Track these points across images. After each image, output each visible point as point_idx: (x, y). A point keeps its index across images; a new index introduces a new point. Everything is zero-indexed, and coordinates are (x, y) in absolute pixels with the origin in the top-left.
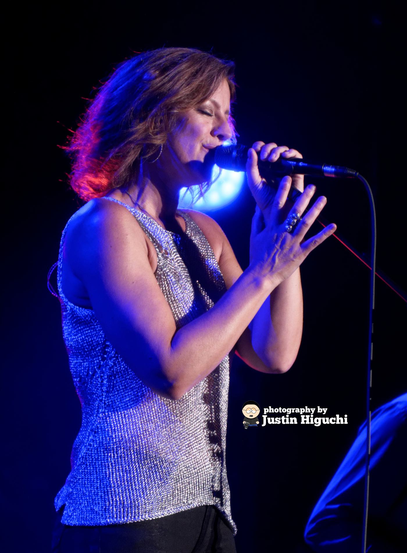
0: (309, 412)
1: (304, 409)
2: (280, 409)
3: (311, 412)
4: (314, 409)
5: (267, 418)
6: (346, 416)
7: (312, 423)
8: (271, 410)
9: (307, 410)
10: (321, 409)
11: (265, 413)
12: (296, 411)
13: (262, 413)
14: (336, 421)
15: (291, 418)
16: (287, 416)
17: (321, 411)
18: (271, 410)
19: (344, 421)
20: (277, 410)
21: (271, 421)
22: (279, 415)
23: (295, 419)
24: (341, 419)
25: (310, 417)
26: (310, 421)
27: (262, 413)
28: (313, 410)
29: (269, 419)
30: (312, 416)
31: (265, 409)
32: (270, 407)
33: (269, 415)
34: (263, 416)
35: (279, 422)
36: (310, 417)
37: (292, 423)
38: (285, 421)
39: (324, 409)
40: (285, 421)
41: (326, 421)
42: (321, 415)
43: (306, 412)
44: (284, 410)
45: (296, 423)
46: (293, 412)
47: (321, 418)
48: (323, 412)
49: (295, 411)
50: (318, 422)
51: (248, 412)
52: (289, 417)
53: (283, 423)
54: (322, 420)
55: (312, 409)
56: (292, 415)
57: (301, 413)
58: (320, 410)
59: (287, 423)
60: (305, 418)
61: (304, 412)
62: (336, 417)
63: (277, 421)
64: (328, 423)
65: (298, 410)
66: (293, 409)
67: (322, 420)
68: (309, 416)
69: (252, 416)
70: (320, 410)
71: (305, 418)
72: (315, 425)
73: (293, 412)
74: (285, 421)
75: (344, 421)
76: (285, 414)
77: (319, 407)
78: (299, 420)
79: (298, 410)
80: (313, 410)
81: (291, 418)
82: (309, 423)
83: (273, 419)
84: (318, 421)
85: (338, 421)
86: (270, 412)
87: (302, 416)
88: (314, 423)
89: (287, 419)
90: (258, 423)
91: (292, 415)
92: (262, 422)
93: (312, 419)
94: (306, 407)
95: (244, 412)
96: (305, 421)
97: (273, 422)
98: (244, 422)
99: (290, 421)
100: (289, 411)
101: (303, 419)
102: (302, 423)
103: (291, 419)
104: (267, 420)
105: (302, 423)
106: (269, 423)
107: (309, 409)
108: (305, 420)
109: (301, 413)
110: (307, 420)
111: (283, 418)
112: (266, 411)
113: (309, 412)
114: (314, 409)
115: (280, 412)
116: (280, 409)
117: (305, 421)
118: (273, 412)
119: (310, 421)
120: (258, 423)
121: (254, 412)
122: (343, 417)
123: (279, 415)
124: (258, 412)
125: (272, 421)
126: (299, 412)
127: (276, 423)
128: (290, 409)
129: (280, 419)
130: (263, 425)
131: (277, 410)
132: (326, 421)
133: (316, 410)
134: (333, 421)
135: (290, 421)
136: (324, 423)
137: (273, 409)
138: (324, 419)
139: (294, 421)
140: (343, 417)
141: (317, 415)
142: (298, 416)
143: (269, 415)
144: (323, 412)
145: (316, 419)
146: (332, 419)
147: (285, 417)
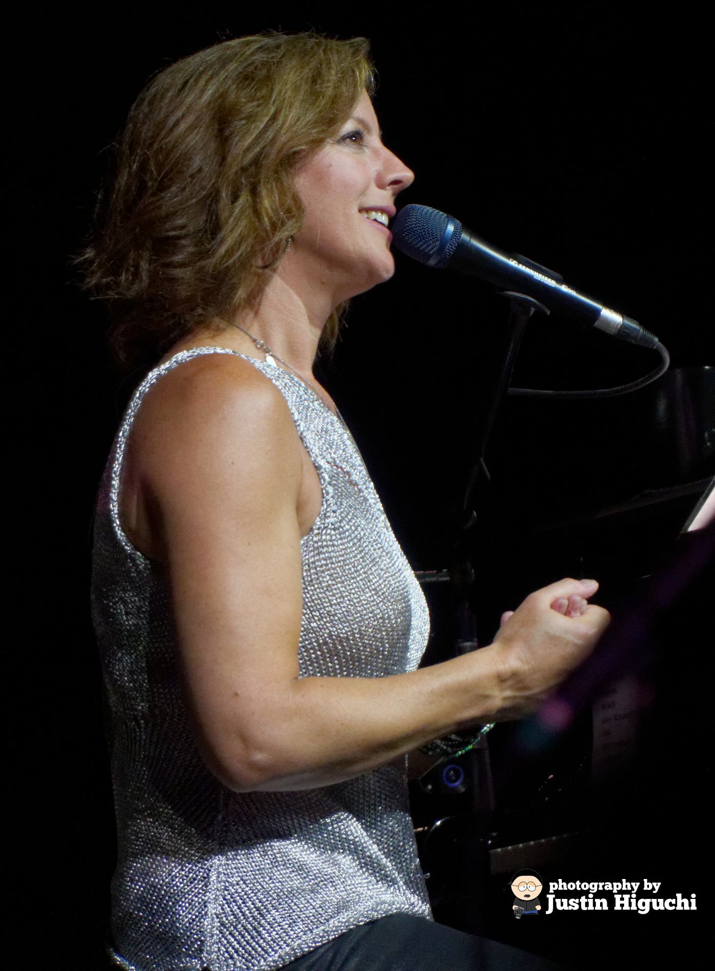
0: (629, 888)
1: (619, 884)
2: (578, 883)
3: (633, 889)
4: (638, 884)
5: (554, 899)
7: (634, 908)
8: (561, 885)
9: (625, 885)
10: (650, 884)
11: (551, 891)
12: (606, 888)
13: (546, 890)
15: (596, 900)
16: (591, 896)
17: (650, 888)
18: (561, 885)
20: (572, 886)
21: (562, 904)
22: (577, 894)
23: (604, 901)
25: (631, 898)
26: (630, 905)
27: (546, 890)
28: (636, 886)
29: (558, 901)
30: (634, 896)
31: (551, 884)
32: (560, 880)
33: (559, 894)
35: (576, 907)
36: (631, 898)
37: (598, 908)
38: (587, 904)
39: (655, 884)
40: (587, 904)
42: (649, 895)
43: (624, 888)
44: (586, 886)
45: (605, 907)
46: (601, 888)
47: (649, 900)
48: (653, 889)
49: (603, 886)
50: (644, 907)
51: (522, 888)
52: (594, 898)
53: (584, 908)
54: (651, 903)
55: (633, 884)
56: (599, 895)
57: (615, 891)
58: (647, 885)
59: (591, 908)
60: (622, 899)
61: (619, 888)
63: (572, 905)
65: (608, 886)
66: (601, 884)
67: (651, 903)
68: (628, 896)
69: (528, 896)
70: (647, 885)
71: (622, 899)
73: (601, 888)
74: (587, 904)
76: (586, 893)
77: (646, 880)
78: (612, 903)
79: (608, 886)
80: (636, 886)
81: (596, 900)
82: (628, 908)
83: (565, 901)
84: (644, 904)
86: (560, 888)
87: (616, 896)
88: (638, 909)
89: (591, 902)
90: (539, 908)
91: (599, 895)
92: (545, 907)
93: (633, 901)
94: (624, 880)
95: (514, 889)
96: (622, 905)
97: (565, 907)
98: (514, 907)
99: (594, 905)
100: (594, 887)
101: (618, 902)
102: (616, 908)
103: (598, 901)
104: (555, 904)
105: (616, 908)
106: (559, 907)
107: (628, 884)
108: (622, 902)
109: (615, 891)
110: (626, 902)
111: (583, 900)
112: (553, 887)
113: (629, 888)
114: (638, 884)
115: (578, 889)
116: (578, 883)
117: (622, 905)
118: (565, 888)
119: (630, 905)
120: (539, 908)
121: (532, 888)
123: (577, 894)
124: (540, 889)
125: (564, 905)
127: (570, 908)
128: (596, 884)
129: (577, 901)
131: (572, 886)
133: (642, 885)
135: (594, 905)
137: (565, 884)
138: (654, 901)
139: (602, 904)
141: (642, 894)
142: (609, 896)
143: (559, 894)
144: (653, 889)
145: (641, 901)
147: (587, 898)
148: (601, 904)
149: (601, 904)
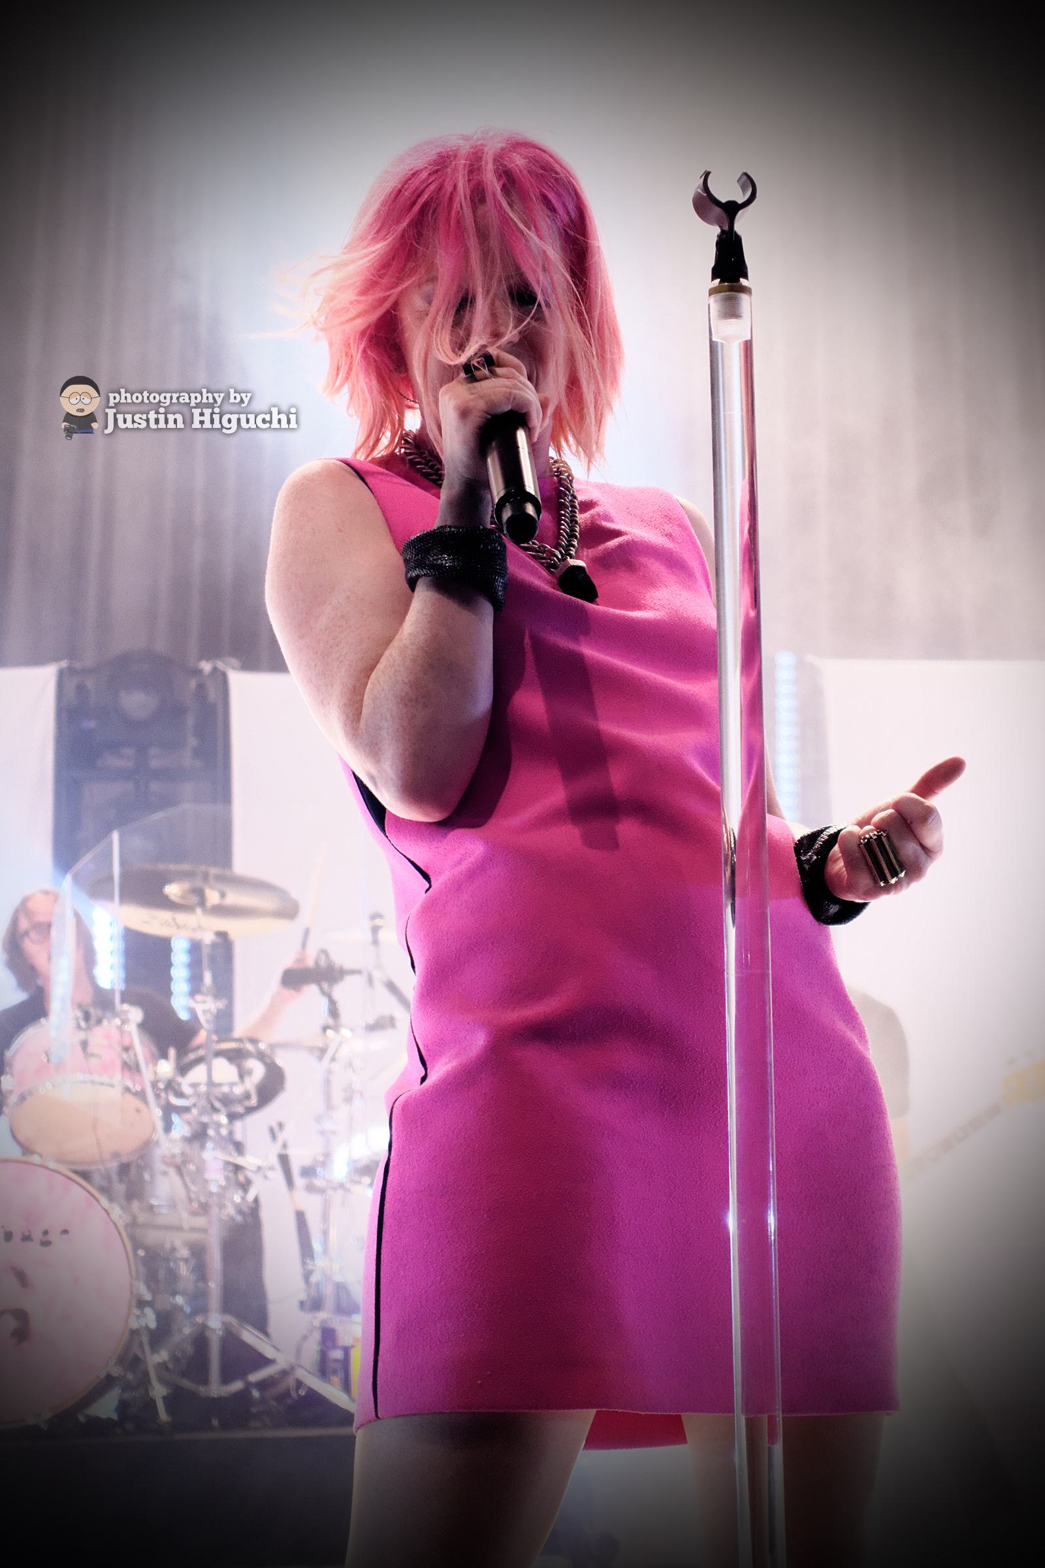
0: (211, 401)
2: (146, 394)
4: (222, 395)
5: (115, 415)
6: (293, 410)
11: (111, 404)
14: (271, 422)
16: (162, 410)
17: (238, 400)
19: (289, 422)
20: (137, 398)
21: (125, 421)
23: (179, 417)
24: (284, 418)
26: (212, 422)
31: (111, 395)
34: (107, 410)
39: (243, 395)
40: (157, 421)
41: (248, 421)
43: (205, 401)
45: (180, 425)
48: (242, 401)
49: (178, 398)
52: (166, 414)
53: (153, 425)
54: (239, 420)
55: (216, 395)
57: (193, 404)
60: (202, 414)
61: (198, 401)
62: (271, 413)
64: (252, 425)
66: (175, 396)
67: (239, 420)
71: (202, 414)
72: (224, 431)
73: (174, 401)
74: (157, 421)
75: (289, 422)
77: (232, 391)
78: (189, 420)
79: (185, 398)
81: (169, 416)
84: (229, 421)
85: (275, 421)
86: (123, 401)
87: (194, 410)
88: (222, 427)
89: (162, 418)
93: (216, 417)
96: (202, 422)
97: (129, 425)
99: (166, 422)
101: (197, 418)
102: (194, 426)
104: (116, 420)
105: (194, 426)
107: (210, 395)
108: (202, 418)
109: (193, 404)
110: (207, 418)
116: (146, 394)
117: (202, 422)
118: (129, 401)
119: (212, 422)
122: (288, 414)
124: (97, 401)
126: (187, 401)
127: (136, 425)
128: (168, 395)
129: (144, 417)
130: (106, 432)
131: (137, 398)
132: (248, 421)
133: (228, 395)
134: (264, 421)
135: (166, 422)
136: (244, 424)
137: (128, 395)
140: (288, 414)
144: (242, 401)
146: (260, 418)
147: (157, 413)
148: (175, 421)
149: (175, 421)
